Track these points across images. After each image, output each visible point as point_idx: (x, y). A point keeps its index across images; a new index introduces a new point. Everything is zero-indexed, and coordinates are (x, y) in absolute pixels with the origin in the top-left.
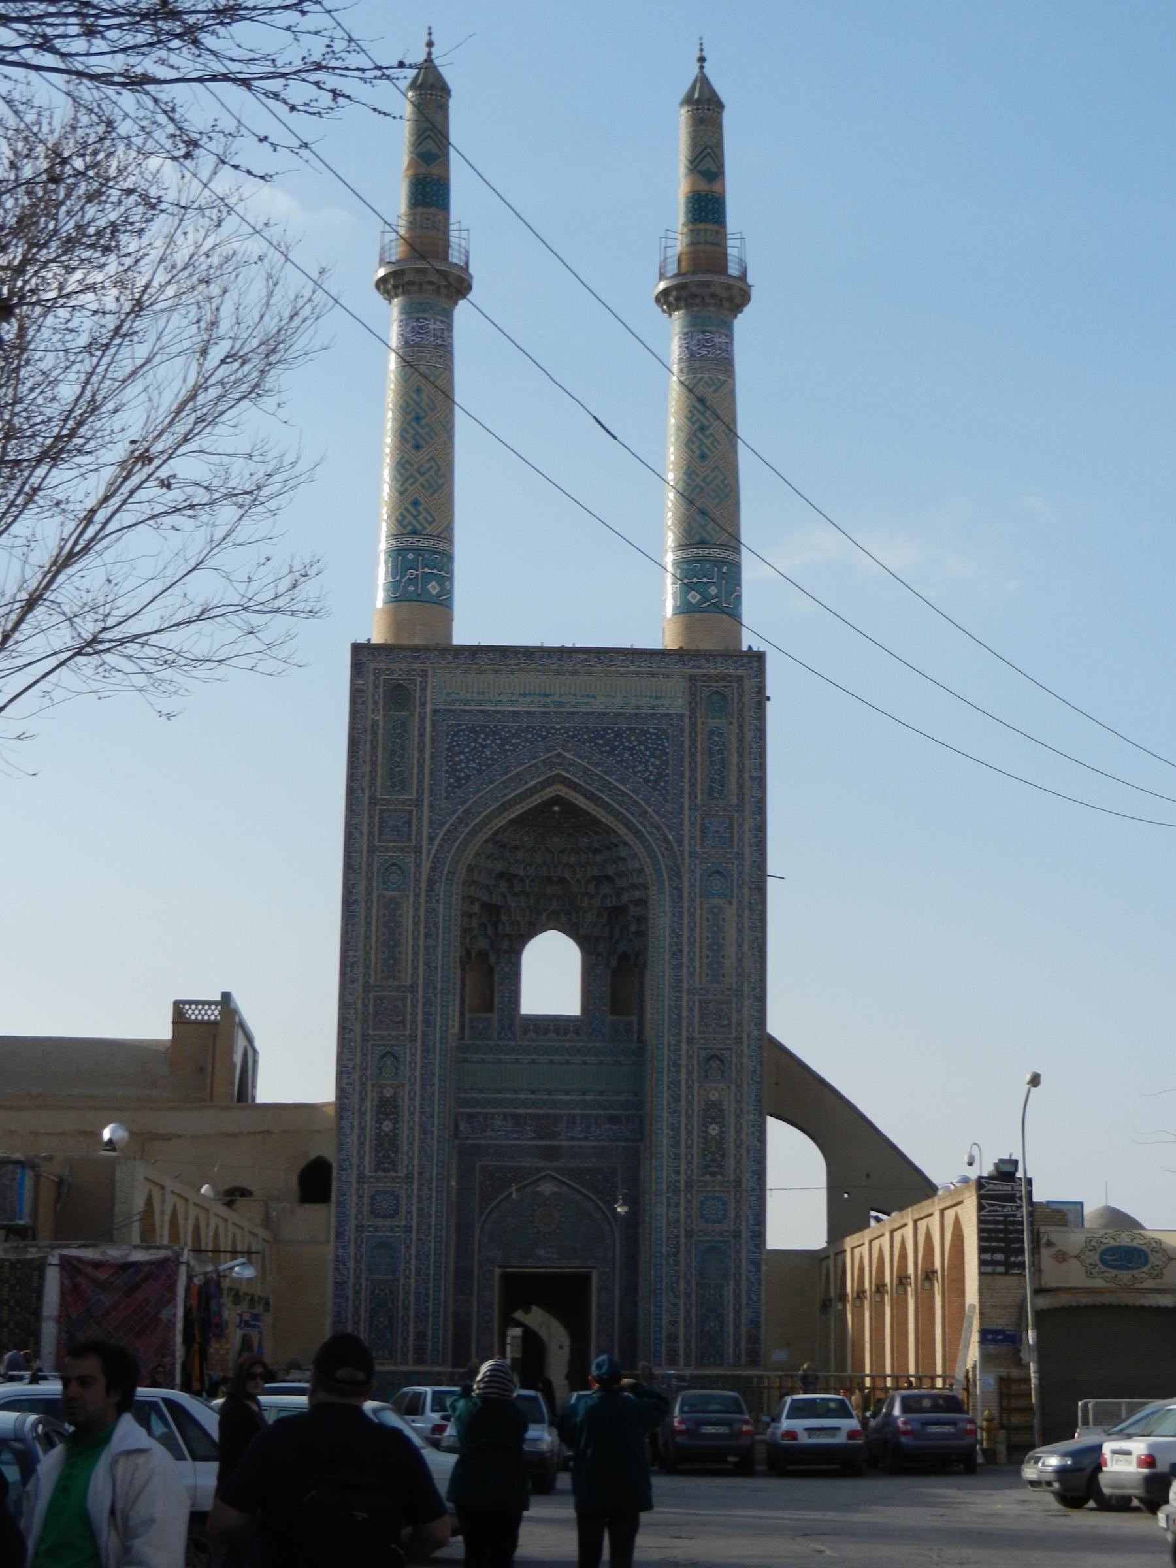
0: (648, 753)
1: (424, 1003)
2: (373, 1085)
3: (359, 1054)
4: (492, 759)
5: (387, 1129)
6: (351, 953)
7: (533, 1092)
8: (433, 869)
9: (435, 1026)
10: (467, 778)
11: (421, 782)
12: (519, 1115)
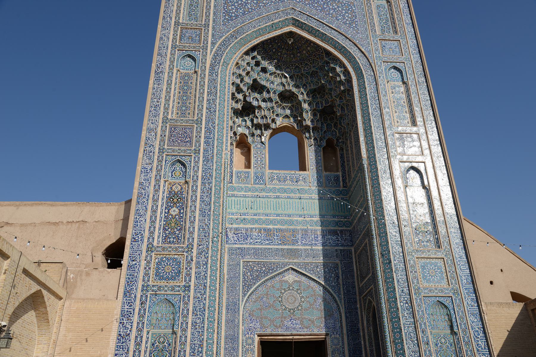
0: (344, 11)
1: (206, 131)
2: (165, 181)
3: (156, 161)
4: (252, 9)
5: (174, 214)
6: (155, 100)
7: (278, 215)
8: (215, 58)
9: (213, 146)
10: (237, 16)
11: (208, 16)
12: (269, 230)
